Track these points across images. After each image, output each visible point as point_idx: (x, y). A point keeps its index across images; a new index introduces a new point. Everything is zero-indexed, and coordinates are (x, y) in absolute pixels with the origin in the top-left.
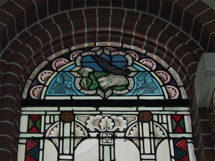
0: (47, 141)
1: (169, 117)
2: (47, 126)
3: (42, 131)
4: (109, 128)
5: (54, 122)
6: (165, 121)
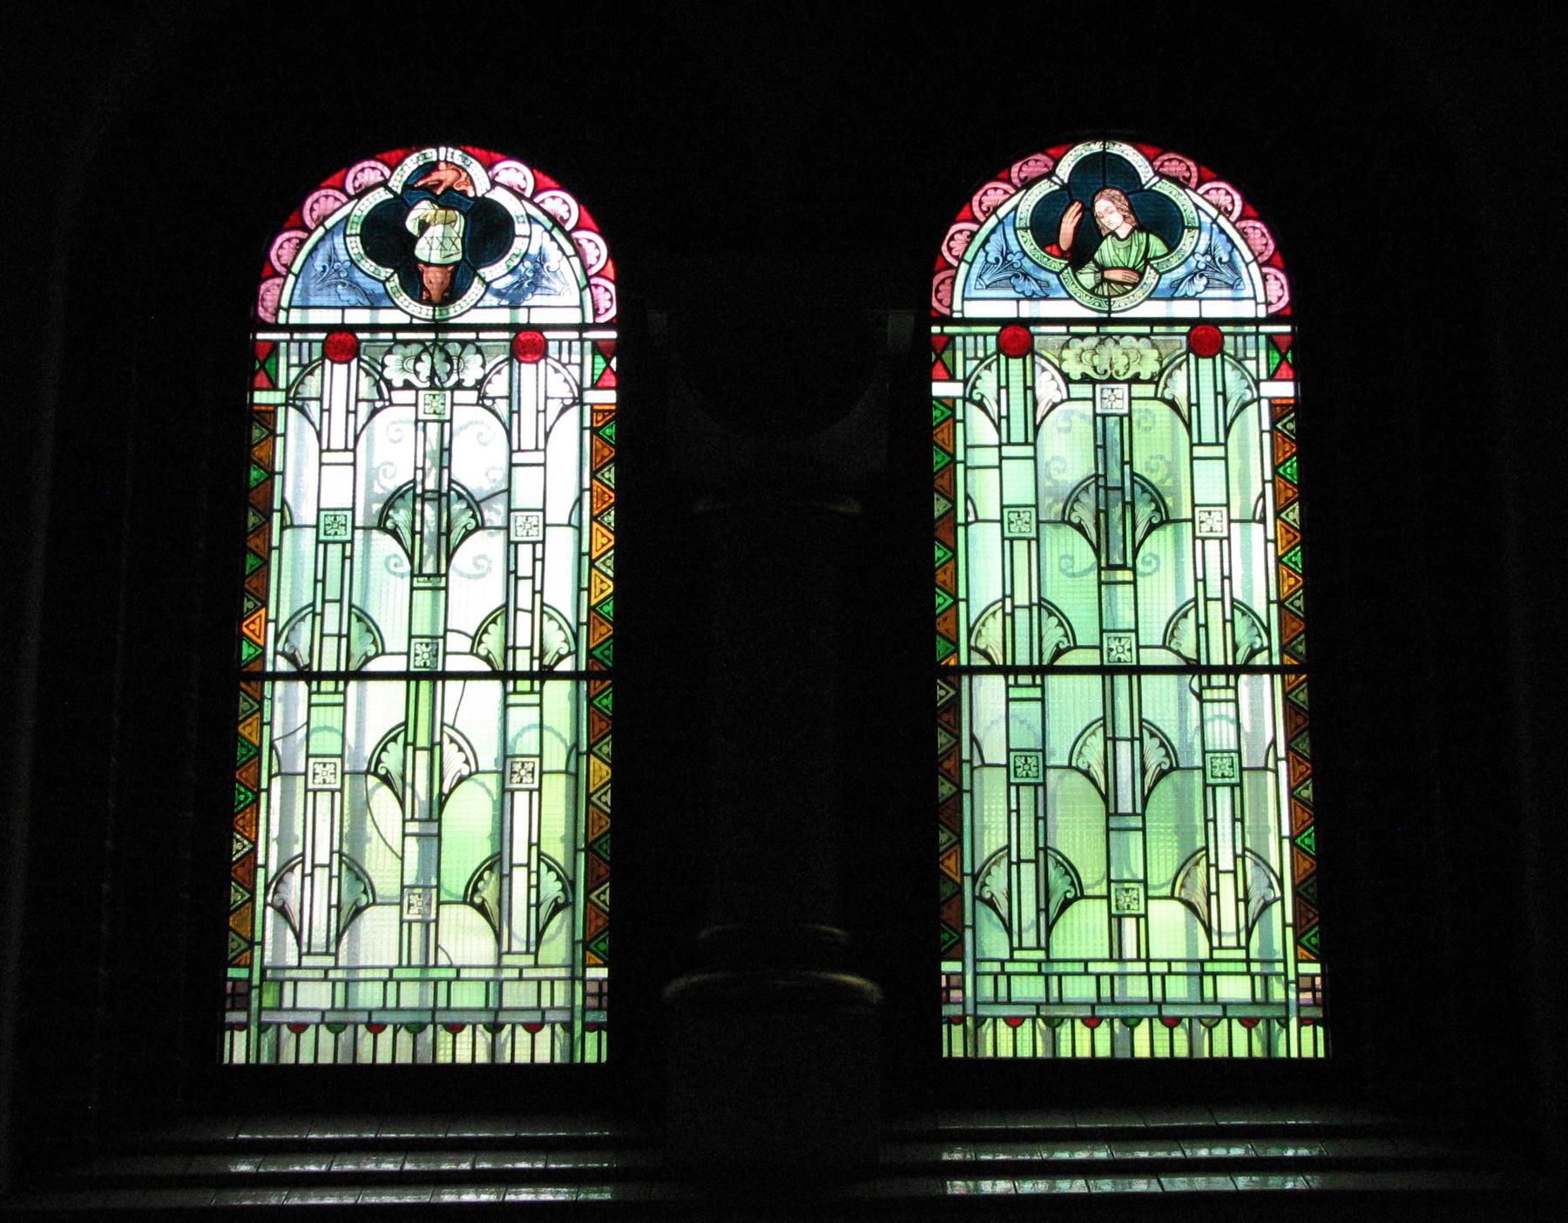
2: (971, 365)
3: (960, 375)
4: (1117, 372)
5: (987, 357)
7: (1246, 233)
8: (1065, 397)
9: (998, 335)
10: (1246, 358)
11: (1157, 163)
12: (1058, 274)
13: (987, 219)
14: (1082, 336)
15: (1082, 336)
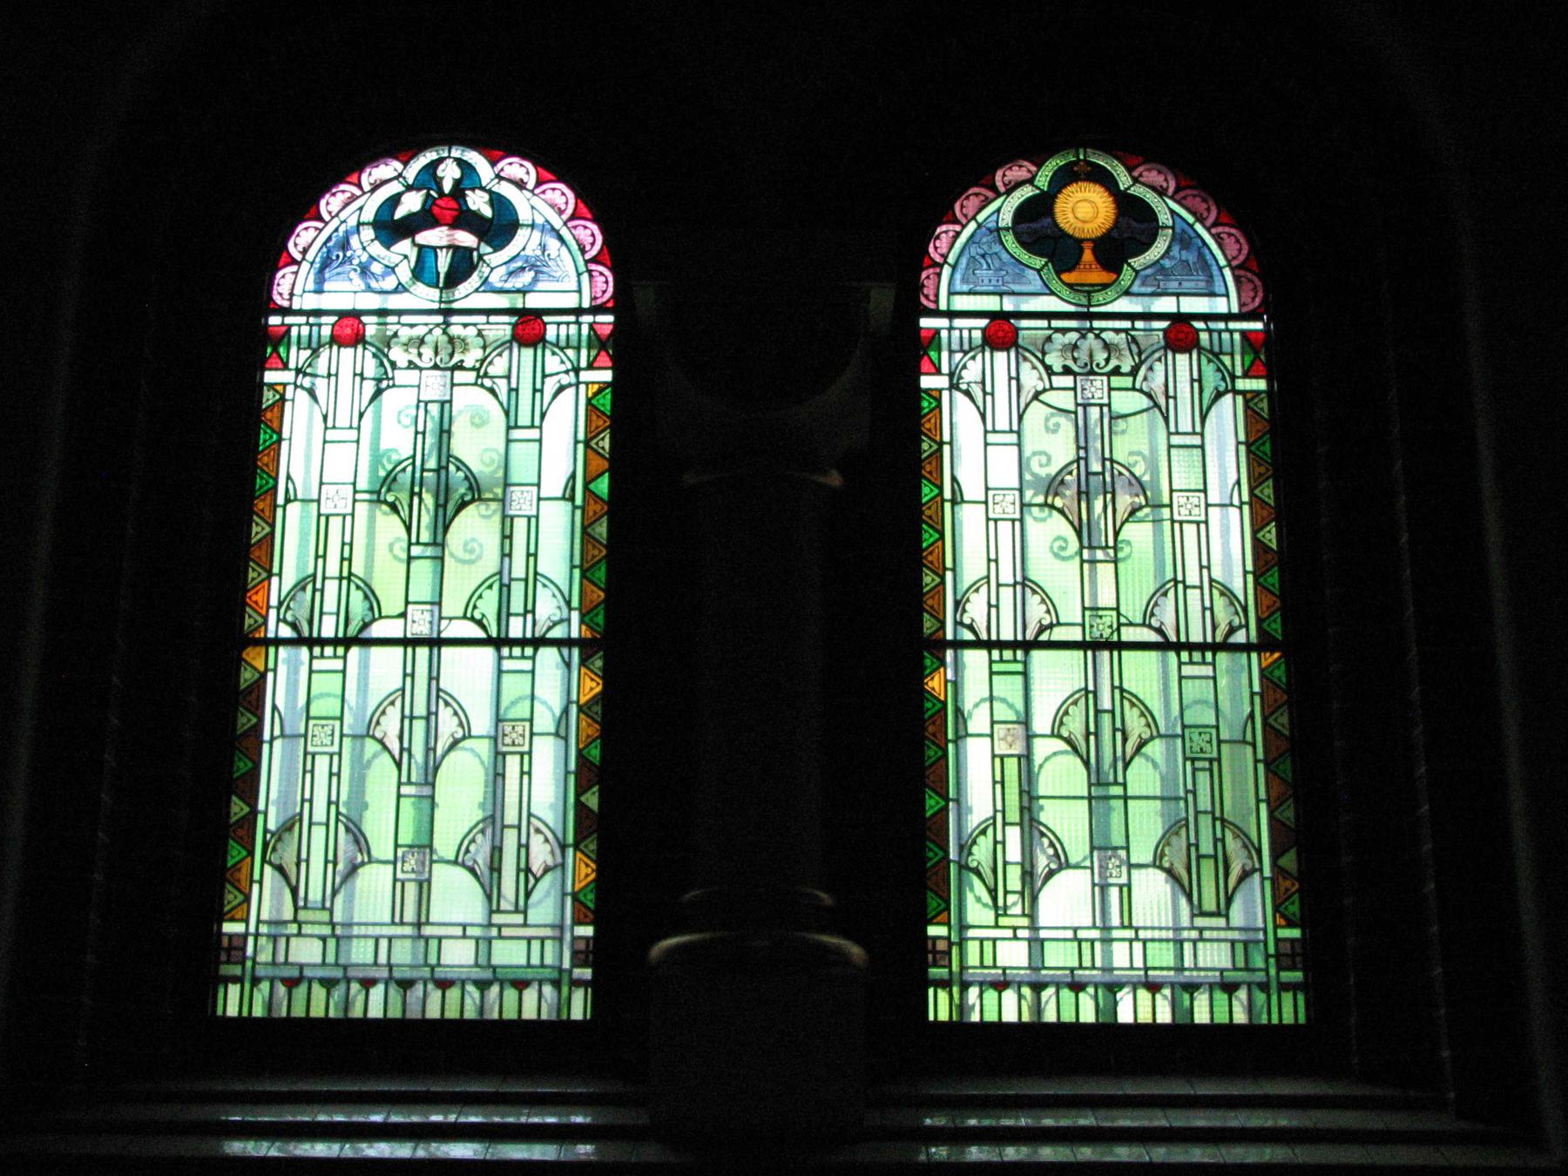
0: (958, 395)
1: (1237, 336)
2: (958, 356)
3: (945, 369)
4: (1098, 365)
6: (1226, 347)
7: (1222, 239)
8: (1048, 386)
9: (984, 330)
10: (1221, 353)
11: (1136, 174)
12: (1039, 271)
14: (1064, 331)
15: (1064, 331)
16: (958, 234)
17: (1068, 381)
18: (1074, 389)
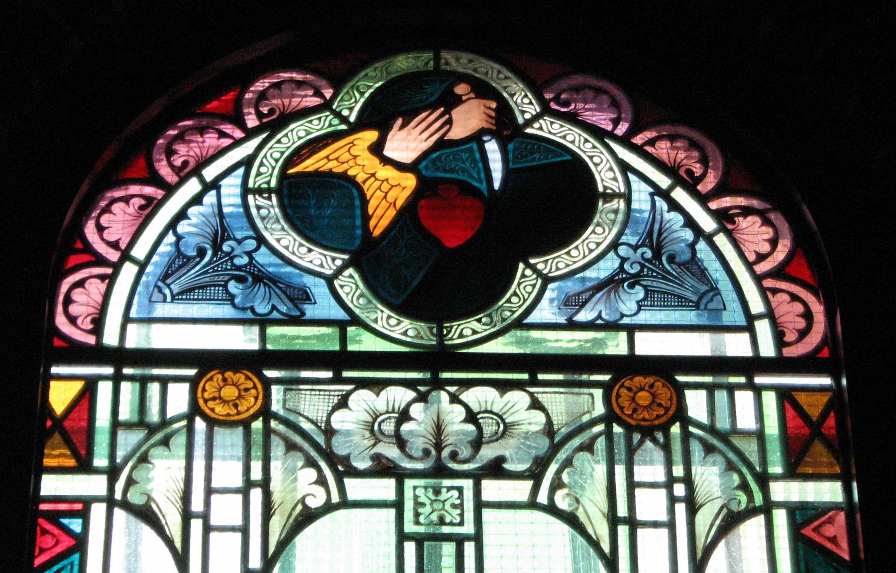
2: (128, 440)
3: (100, 461)
4: (454, 456)
8: (335, 498)
13: (182, 181)
16: (151, 207)
17: (385, 488)
18: (398, 505)
